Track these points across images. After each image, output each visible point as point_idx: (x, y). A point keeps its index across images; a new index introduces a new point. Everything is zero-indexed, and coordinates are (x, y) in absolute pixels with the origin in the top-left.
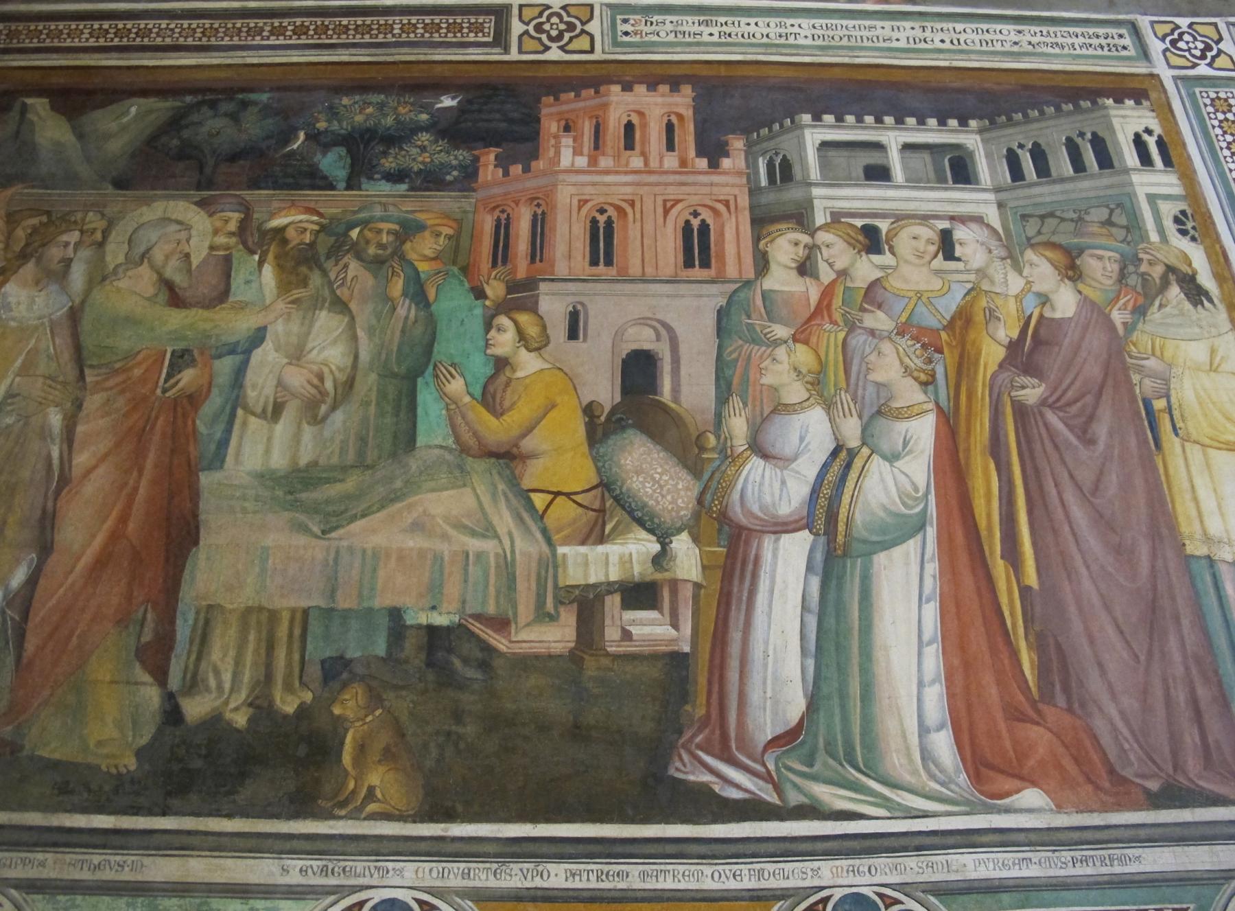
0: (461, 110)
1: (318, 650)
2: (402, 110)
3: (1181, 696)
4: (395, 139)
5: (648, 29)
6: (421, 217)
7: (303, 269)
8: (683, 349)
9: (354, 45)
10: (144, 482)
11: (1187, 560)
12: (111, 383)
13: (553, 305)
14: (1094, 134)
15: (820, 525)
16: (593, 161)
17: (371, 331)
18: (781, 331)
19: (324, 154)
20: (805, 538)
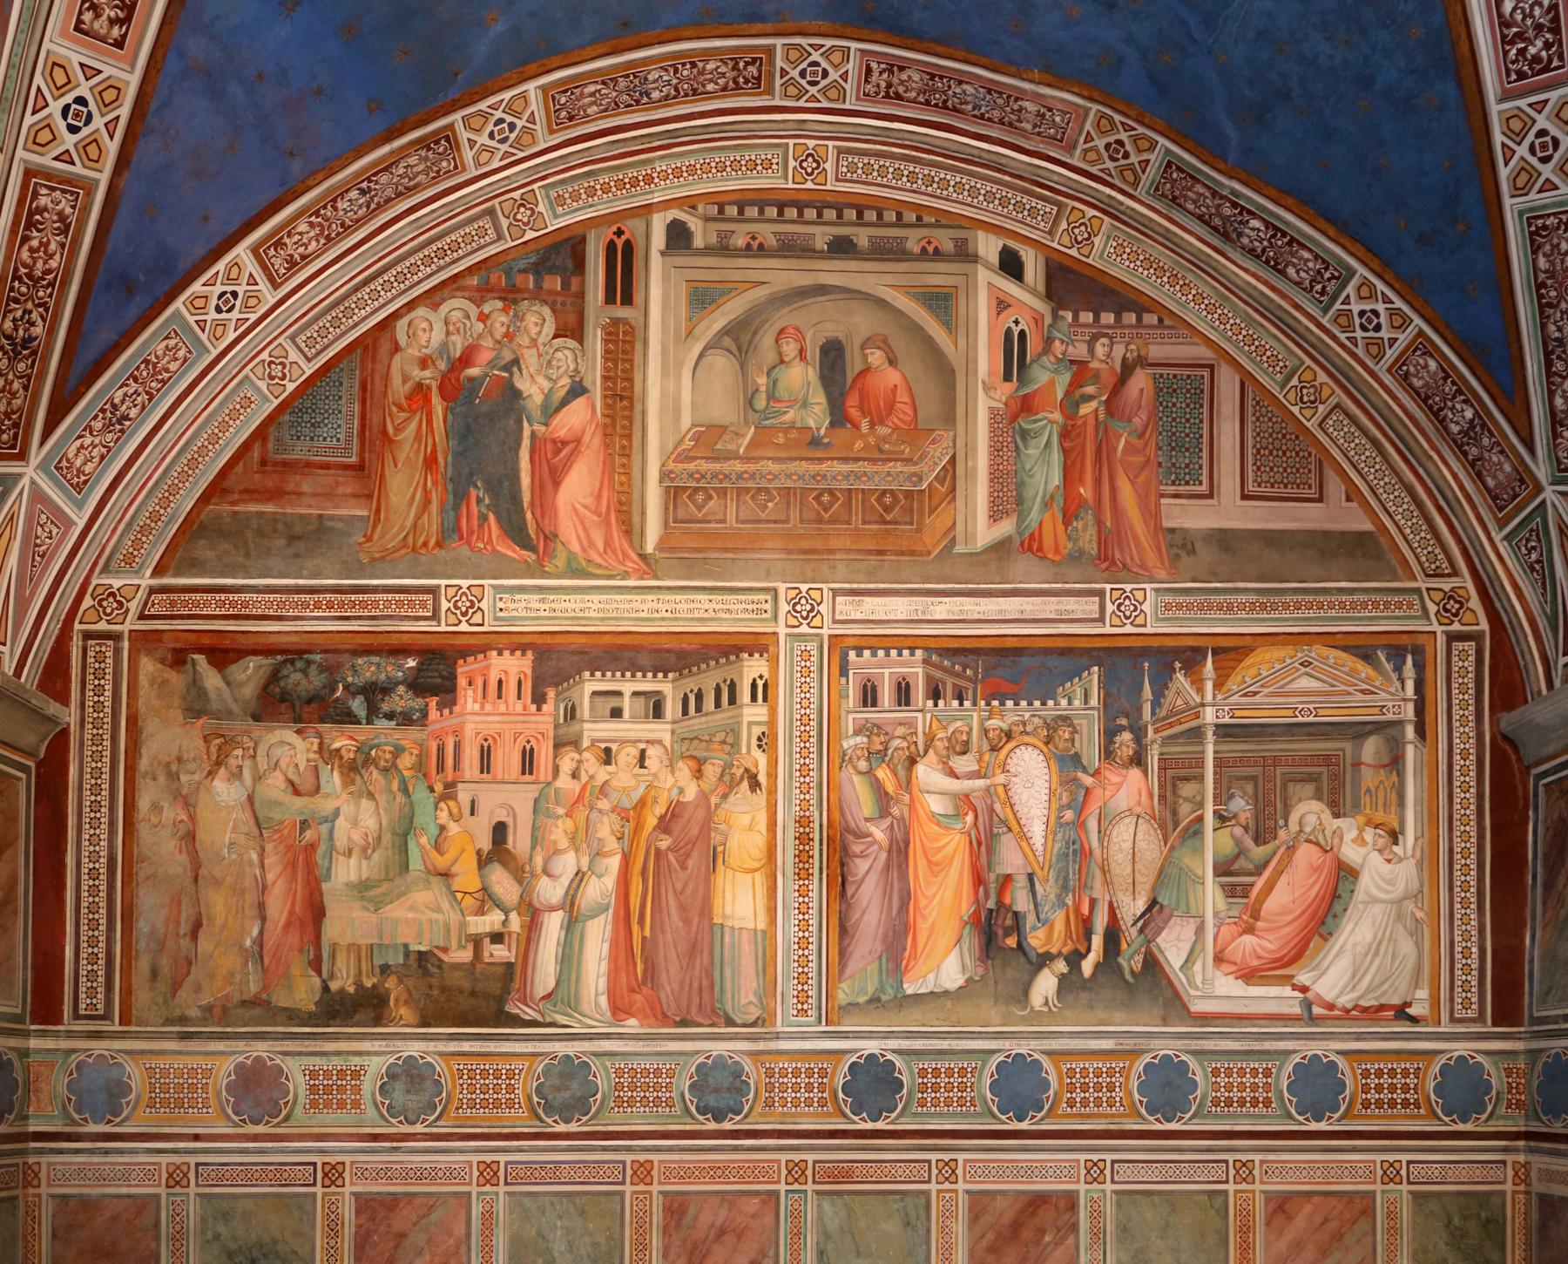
0: (419, 669)
1: (378, 961)
2: (389, 669)
3: (696, 984)
4: (386, 691)
5: (512, 606)
6: (403, 742)
7: (352, 774)
8: (519, 819)
9: (360, 618)
10: (299, 887)
11: (712, 925)
12: (275, 837)
13: (464, 795)
14: (732, 680)
15: (567, 908)
16: (482, 707)
17: (386, 810)
18: (561, 811)
19: (354, 699)
20: (560, 913)
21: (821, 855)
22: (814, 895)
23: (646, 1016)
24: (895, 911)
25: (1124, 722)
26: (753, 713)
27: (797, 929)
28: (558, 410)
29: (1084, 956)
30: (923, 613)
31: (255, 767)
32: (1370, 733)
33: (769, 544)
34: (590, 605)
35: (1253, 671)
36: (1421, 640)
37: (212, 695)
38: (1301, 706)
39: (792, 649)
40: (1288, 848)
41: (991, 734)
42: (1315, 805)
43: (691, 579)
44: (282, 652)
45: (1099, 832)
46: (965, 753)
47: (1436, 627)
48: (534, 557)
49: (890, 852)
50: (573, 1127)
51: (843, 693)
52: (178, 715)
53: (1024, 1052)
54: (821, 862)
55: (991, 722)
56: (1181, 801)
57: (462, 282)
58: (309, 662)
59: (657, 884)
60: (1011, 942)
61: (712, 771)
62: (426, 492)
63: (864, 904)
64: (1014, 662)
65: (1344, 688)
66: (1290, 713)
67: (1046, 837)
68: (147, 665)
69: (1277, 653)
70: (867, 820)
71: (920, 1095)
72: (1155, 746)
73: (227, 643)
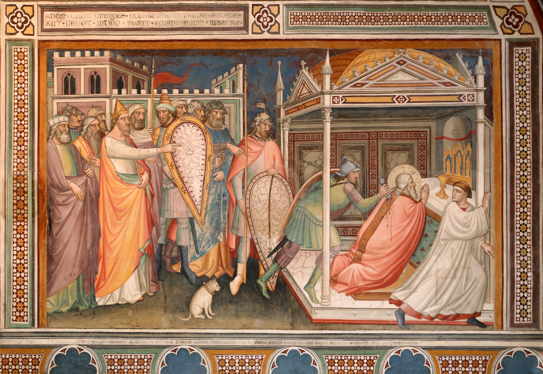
21: (33, 204)
22: (28, 233)
24: (89, 245)
25: (262, 106)
27: (15, 257)
29: (232, 279)
30: (110, 23)
32: (451, 115)
35: (361, 68)
36: (489, 45)
38: (398, 95)
39: (10, 51)
40: (387, 200)
41: (161, 115)
42: (408, 168)
45: (243, 187)
46: (141, 129)
47: (501, 36)
49: (85, 201)
51: (50, 84)
53: (187, 347)
54: (33, 209)
55: (161, 105)
56: (306, 165)
60: (177, 268)
63: (66, 240)
64: (179, 60)
65: (430, 81)
66: (389, 99)
67: (203, 191)
69: (379, 54)
70: (68, 178)
72: (287, 124)
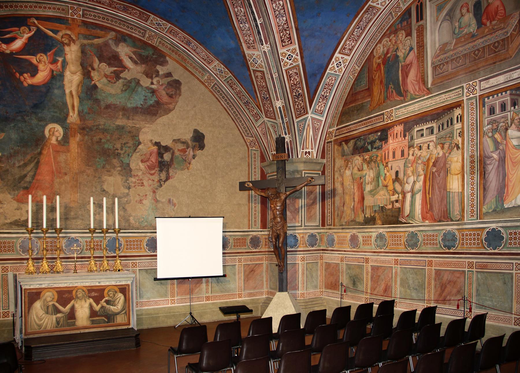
0: (381, 135)
1: (374, 210)
3: (443, 210)
5: (399, 113)
9: (370, 125)
13: (390, 165)
14: (451, 118)
21: (477, 166)
23: (430, 220)
24: (501, 180)
26: (457, 126)
28: (407, 57)
31: (352, 166)
33: (461, 73)
34: (416, 107)
37: (346, 151)
39: (468, 103)
43: (440, 91)
44: (357, 138)
48: (403, 98)
49: (499, 161)
50: (414, 251)
52: (340, 157)
57: (386, 34)
58: (361, 139)
59: (433, 182)
61: (446, 146)
62: (381, 90)
63: (491, 180)
68: (336, 147)
70: (492, 152)
71: (510, 241)
73: (348, 138)
